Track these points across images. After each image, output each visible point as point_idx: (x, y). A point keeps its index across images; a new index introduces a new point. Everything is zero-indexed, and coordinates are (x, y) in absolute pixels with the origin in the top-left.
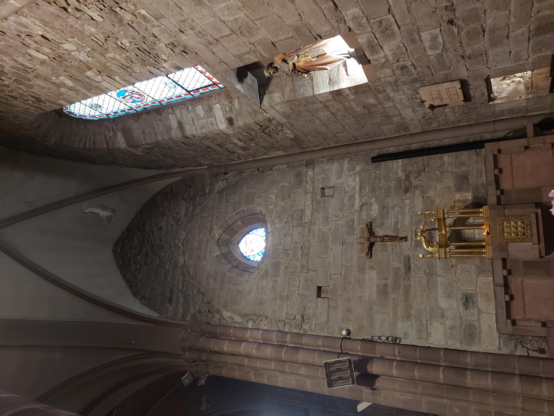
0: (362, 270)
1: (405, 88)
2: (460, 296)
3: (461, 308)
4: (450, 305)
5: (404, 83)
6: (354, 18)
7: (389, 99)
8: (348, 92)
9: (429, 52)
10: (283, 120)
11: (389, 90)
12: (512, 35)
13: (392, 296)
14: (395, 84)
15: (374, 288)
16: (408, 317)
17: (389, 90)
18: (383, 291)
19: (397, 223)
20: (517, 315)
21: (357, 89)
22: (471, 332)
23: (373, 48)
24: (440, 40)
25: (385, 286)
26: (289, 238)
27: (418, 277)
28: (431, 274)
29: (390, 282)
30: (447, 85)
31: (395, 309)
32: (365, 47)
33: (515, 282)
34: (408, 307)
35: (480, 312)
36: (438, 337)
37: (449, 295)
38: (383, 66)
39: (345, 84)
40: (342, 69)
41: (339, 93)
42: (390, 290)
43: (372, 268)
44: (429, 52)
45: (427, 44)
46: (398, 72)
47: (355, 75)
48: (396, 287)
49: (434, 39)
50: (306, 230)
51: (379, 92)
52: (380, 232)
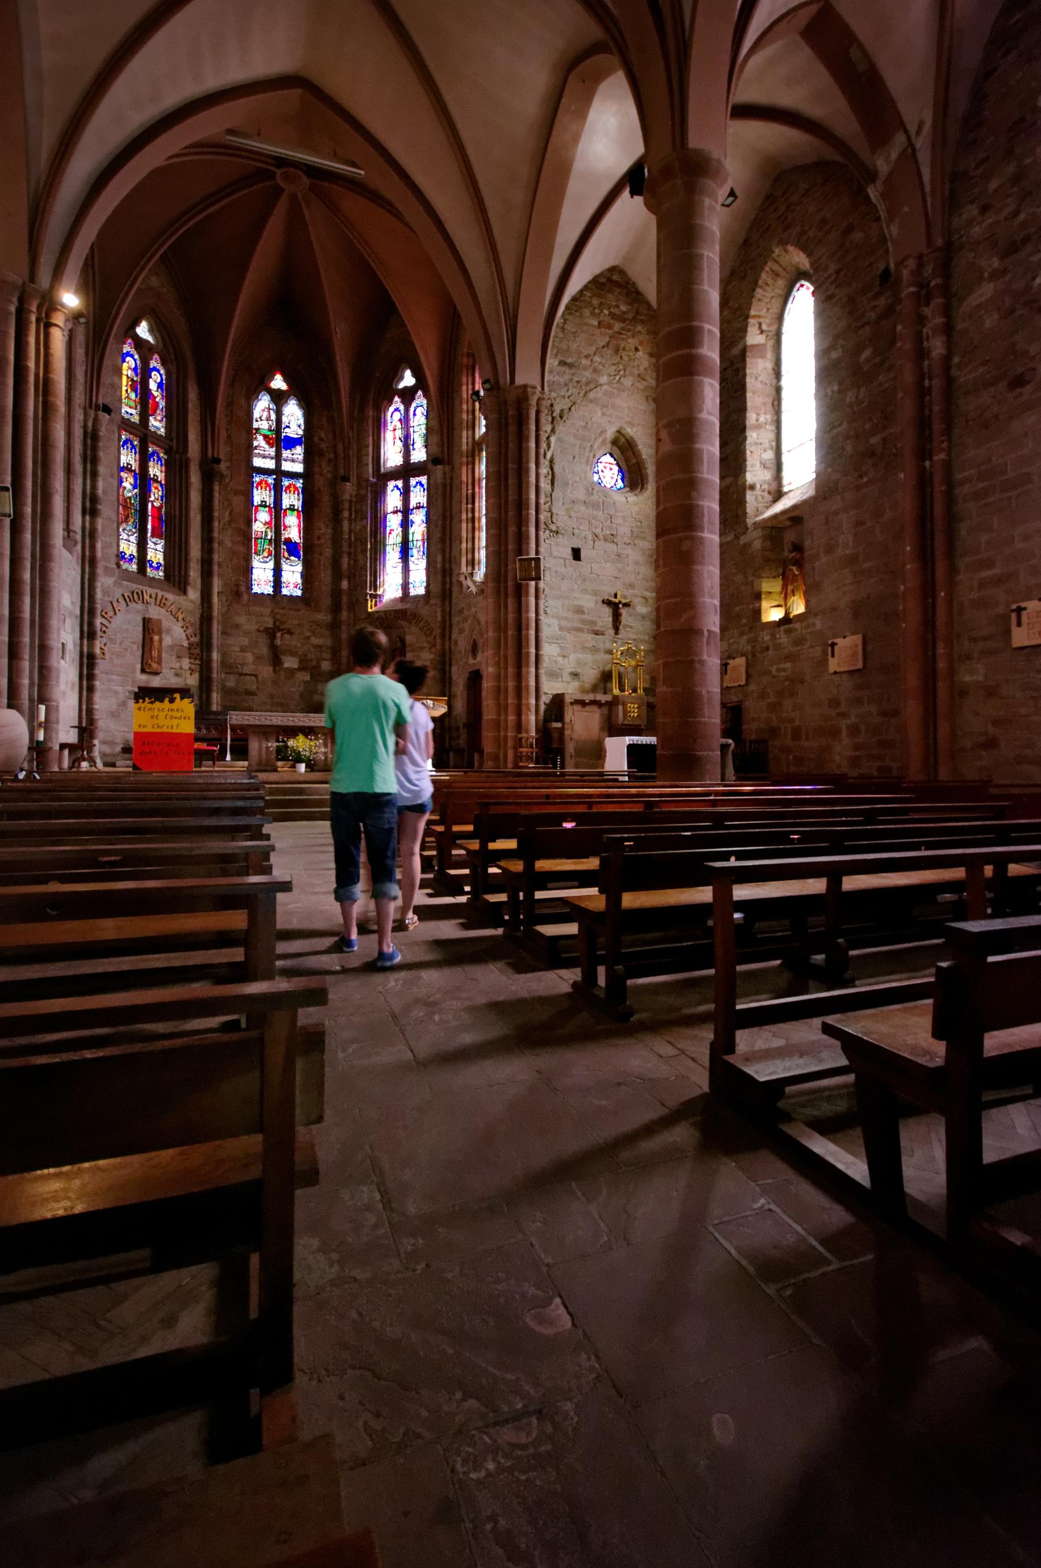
0: (595, 593)
1: (749, 648)
2: (579, 670)
3: (570, 670)
4: (569, 664)
5: (754, 647)
6: (814, 624)
7: (742, 634)
8: (757, 605)
9: (775, 667)
10: (743, 540)
11: (751, 635)
12: (773, 715)
13: (577, 616)
14: (754, 640)
15: (581, 603)
16: (561, 628)
17: (751, 635)
18: (579, 610)
19: (631, 627)
20: (575, 707)
21: (758, 612)
22: (554, 675)
23: (788, 632)
24: (782, 674)
25: (583, 613)
26: (621, 521)
27: (590, 639)
28: (594, 650)
29: (587, 617)
30: (744, 676)
31: (566, 619)
32: (791, 626)
33: (595, 708)
34: (569, 630)
35: (568, 683)
36: (549, 650)
37: (579, 662)
38: (773, 636)
39: (765, 604)
40: (776, 603)
41: (758, 597)
42: (580, 616)
43: (596, 602)
44: (775, 667)
45: (781, 666)
46: (765, 645)
47: (773, 614)
48: (584, 622)
49: (784, 670)
50: (628, 541)
51: (751, 628)
52: (624, 611)
